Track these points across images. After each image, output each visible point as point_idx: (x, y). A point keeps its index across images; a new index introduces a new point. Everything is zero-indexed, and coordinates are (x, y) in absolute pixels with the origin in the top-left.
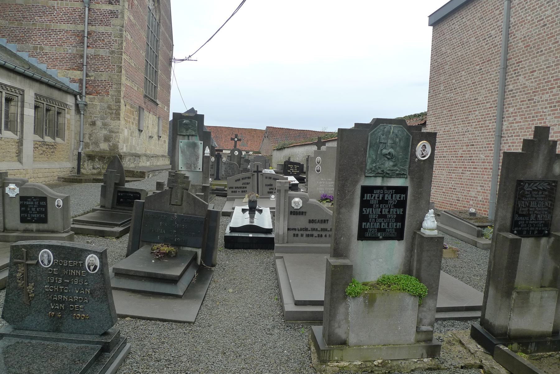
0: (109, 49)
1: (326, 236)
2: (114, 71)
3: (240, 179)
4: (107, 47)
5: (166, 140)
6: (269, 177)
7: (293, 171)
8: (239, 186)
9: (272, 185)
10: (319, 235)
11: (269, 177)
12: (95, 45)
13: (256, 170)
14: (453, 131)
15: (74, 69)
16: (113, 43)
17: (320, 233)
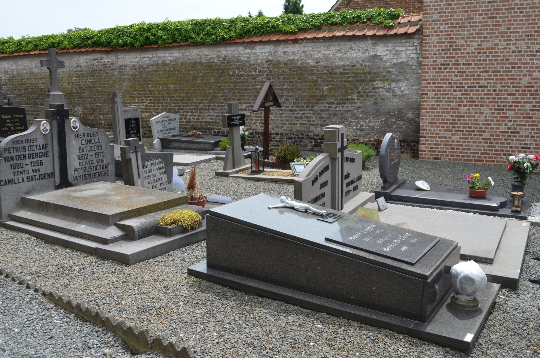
7: (12, 128)
14: (505, 48)
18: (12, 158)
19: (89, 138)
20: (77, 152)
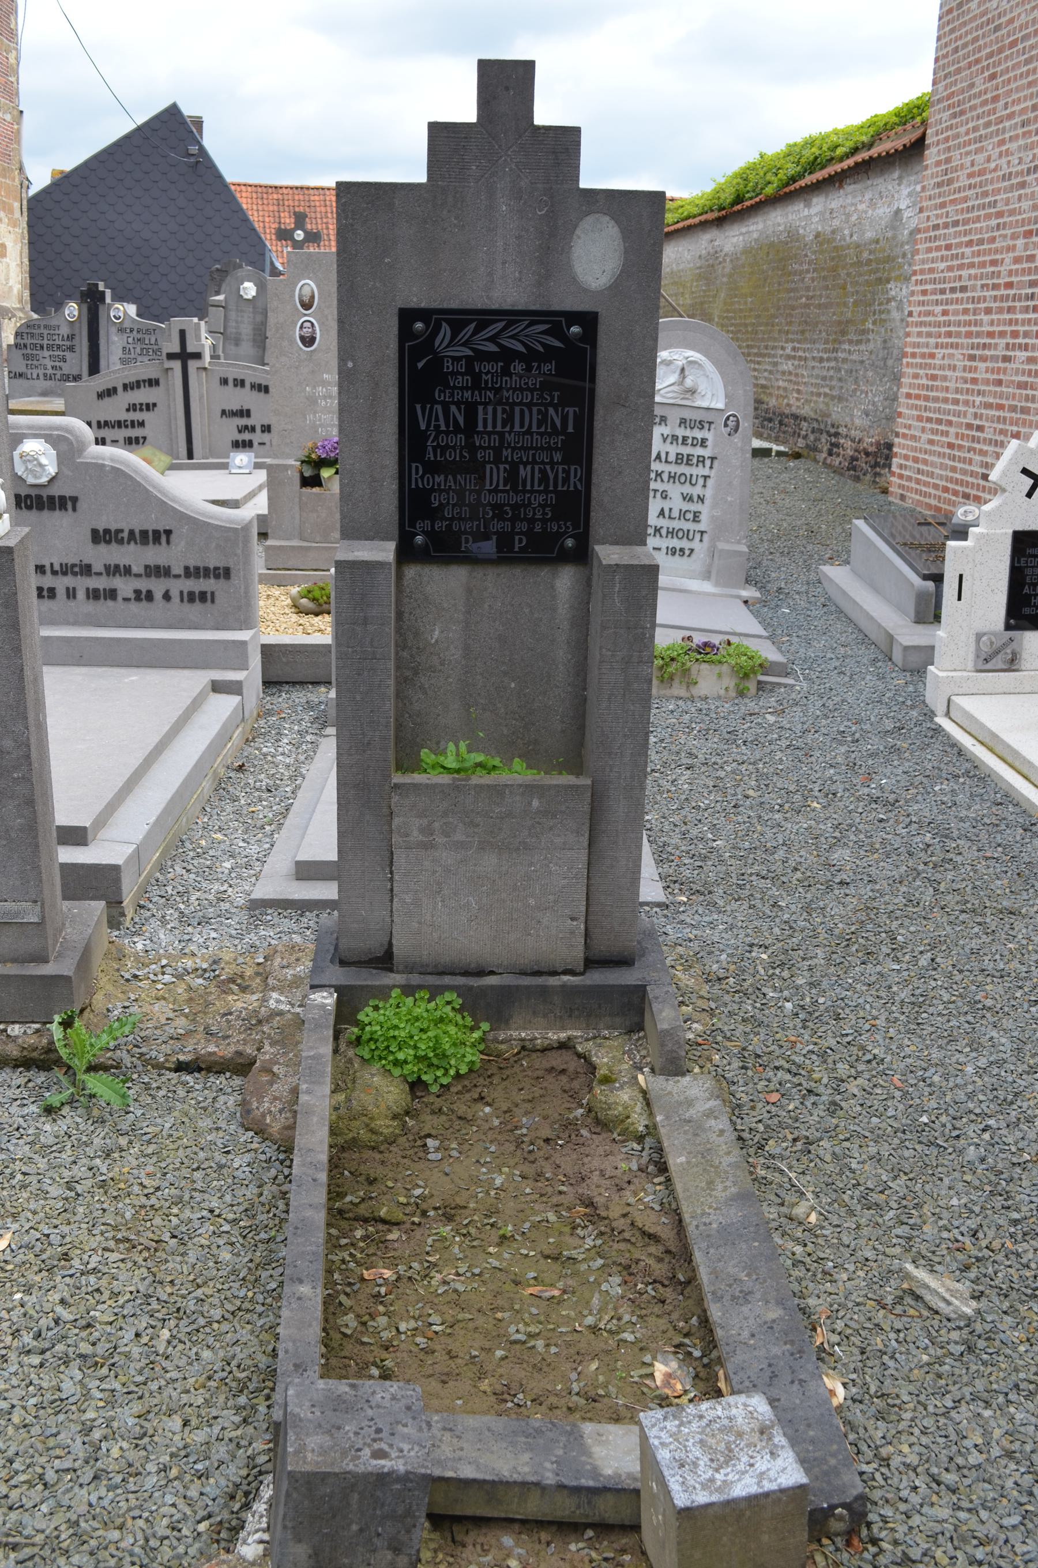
1: (167, 597)
3: (115, 389)
5: (9, 245)
6: (235, 380)
8: (112, 418)
9: (248, 413)
10: (138, 592)
11: (235, 380)
13: (176, 348)
17: (143, 585)
18: (25, 346)
19: (139, 336)
20: (119, 353)
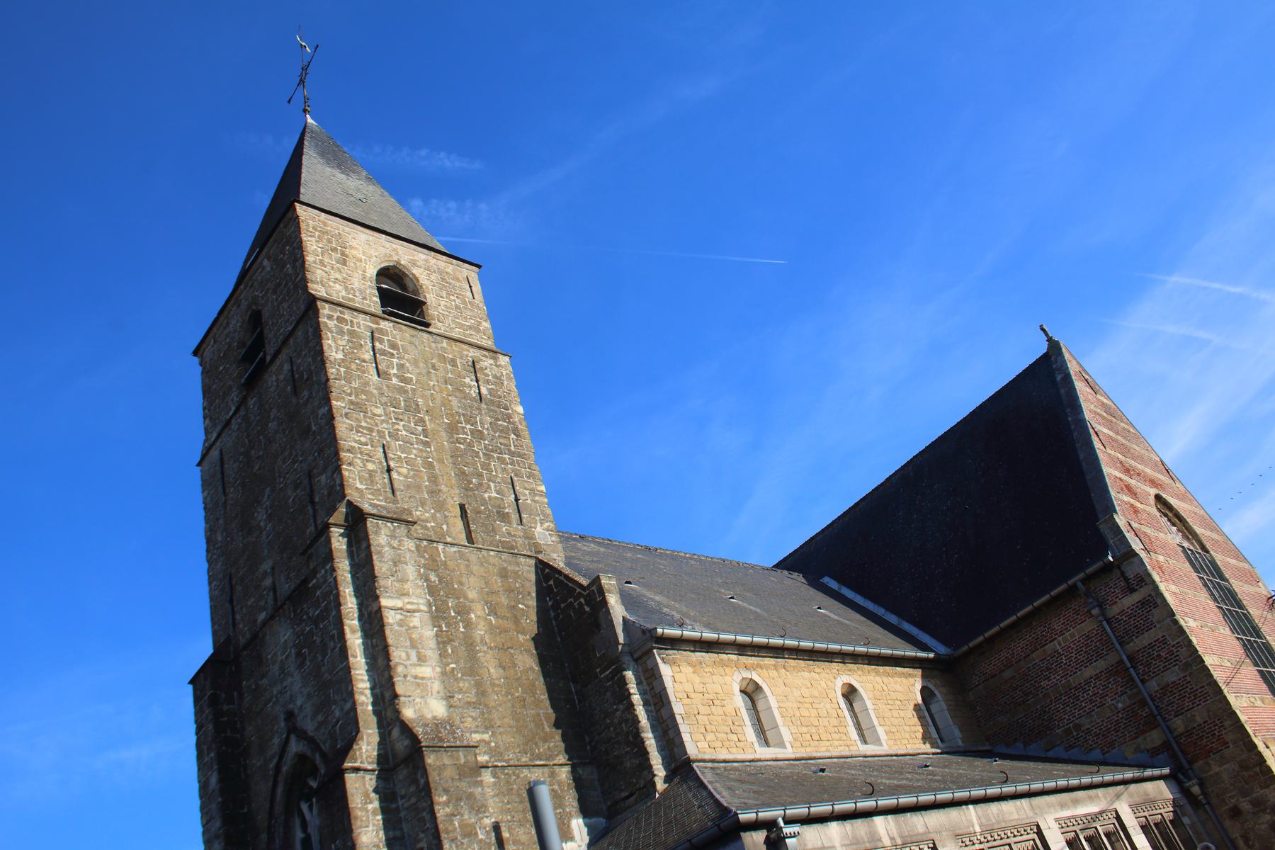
0: (1176, 664)
2: (1209, 696)
4: (1172, 663)
12: (1150, 671)
15: (1144, 732)
16: (1176, 652)
